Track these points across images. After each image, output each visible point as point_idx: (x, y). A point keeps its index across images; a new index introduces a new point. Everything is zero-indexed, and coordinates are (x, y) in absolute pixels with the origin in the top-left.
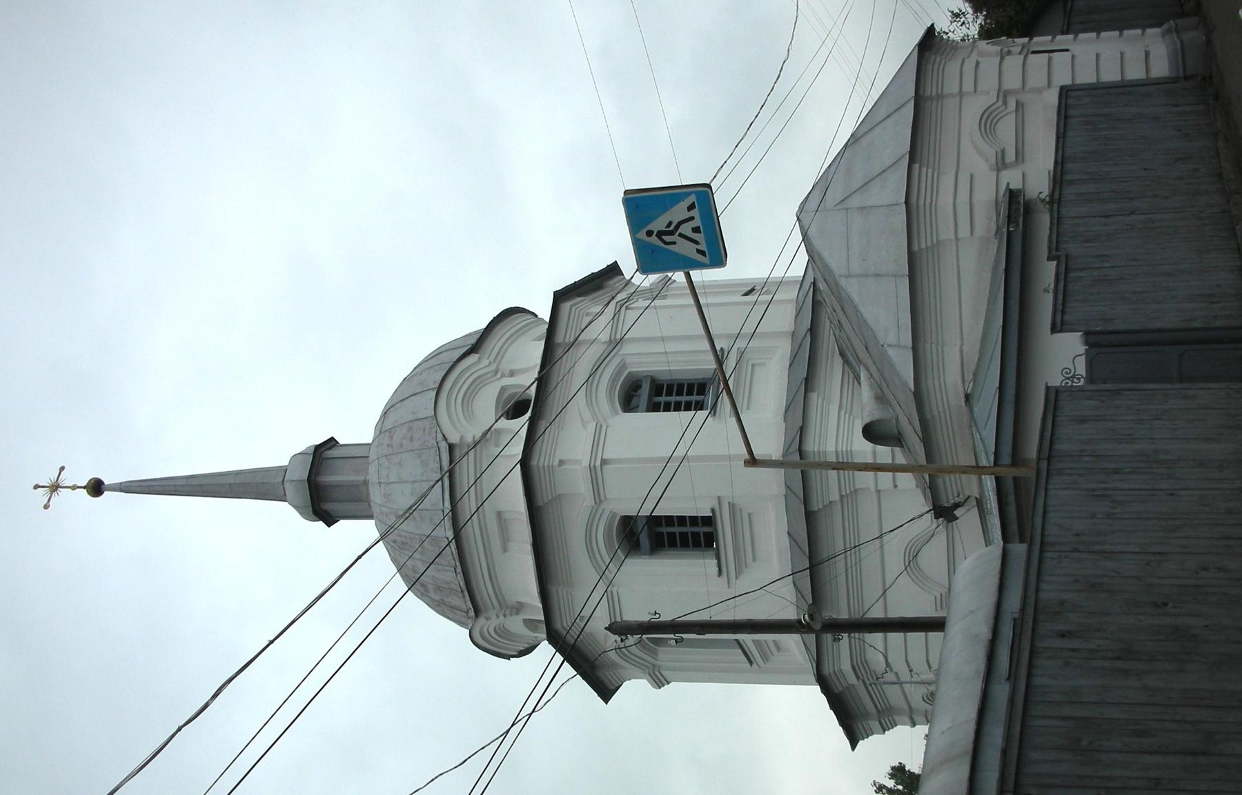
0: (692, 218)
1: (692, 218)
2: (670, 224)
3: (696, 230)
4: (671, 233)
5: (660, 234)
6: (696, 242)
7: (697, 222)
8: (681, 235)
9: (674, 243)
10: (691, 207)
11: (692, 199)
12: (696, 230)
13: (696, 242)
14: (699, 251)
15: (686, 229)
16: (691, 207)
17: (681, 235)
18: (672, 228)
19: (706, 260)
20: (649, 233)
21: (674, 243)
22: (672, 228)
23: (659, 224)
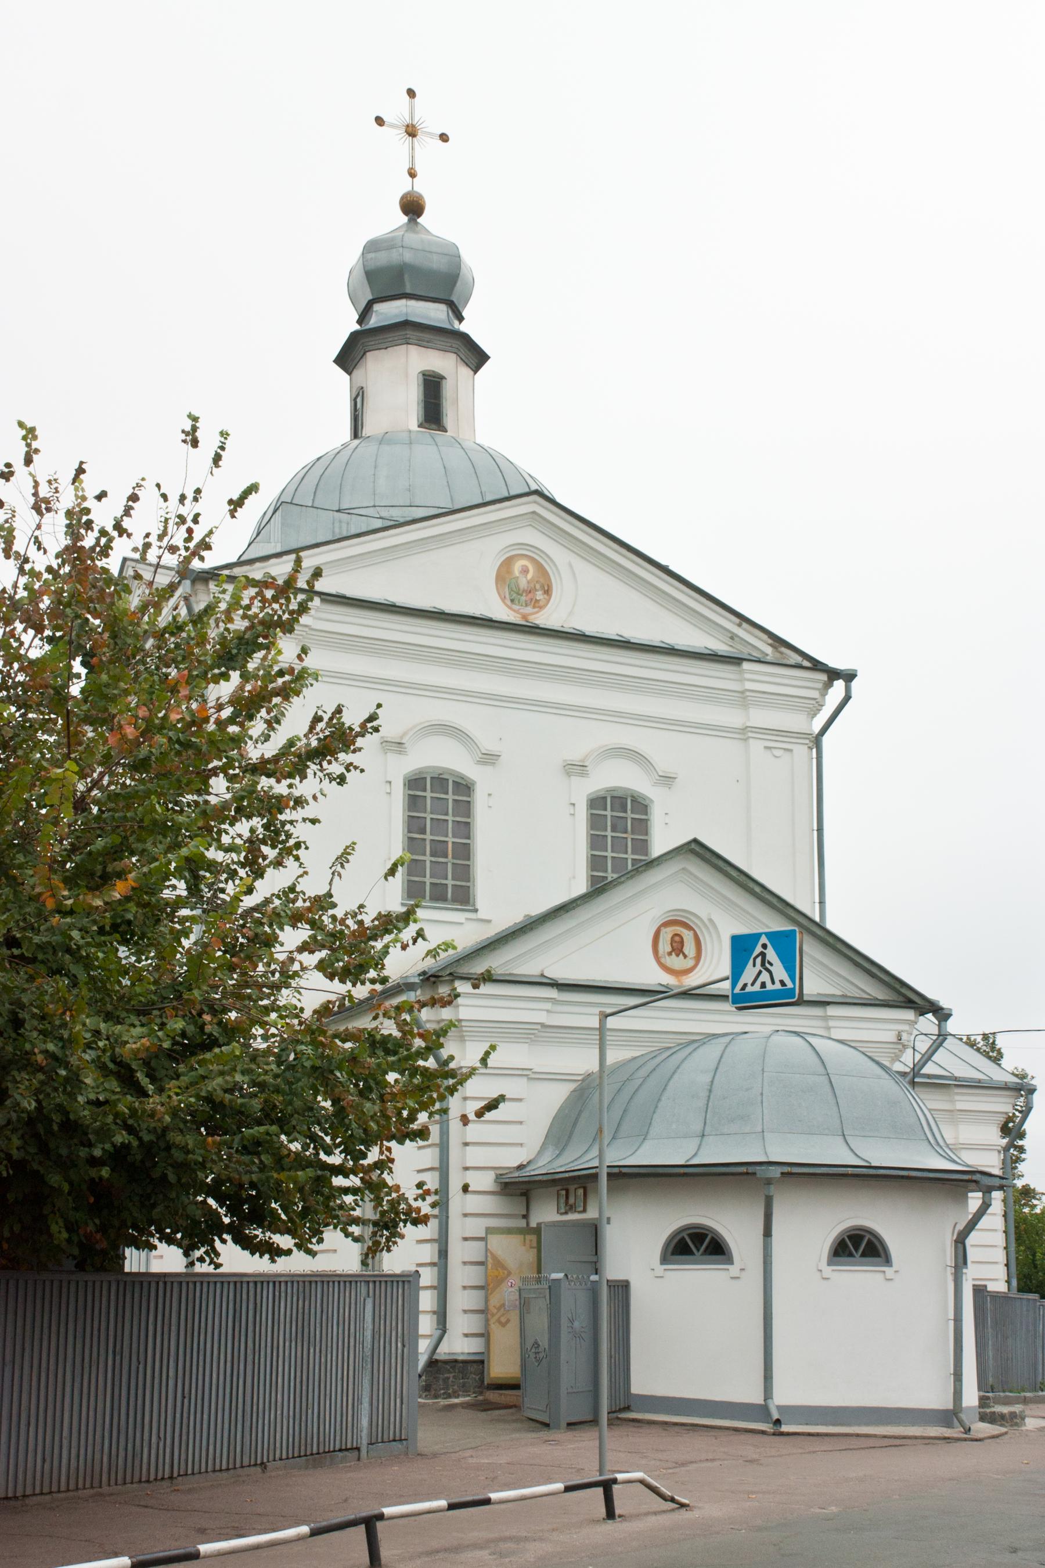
0: (773, 982)
1: (773, 982)
2: (771, 964)
3: (763, 985)
4: (763, 964)
5: (763, 955)
6: (753, 984)
7: (769, 986)
8: (760, 972)
9: (754, 965)
10: (782, 983)
11: (790, 985)
12: (763, 985)
13: (753, 984)
14: (745, 985)
15: (765, 977)
16: (782, 983)
17: (760, 972)
18: (767, 965)
19: (737, 990)
20: (764, 946)
21: (754, 965)
22: (767, 965)
23: (771, 954)
